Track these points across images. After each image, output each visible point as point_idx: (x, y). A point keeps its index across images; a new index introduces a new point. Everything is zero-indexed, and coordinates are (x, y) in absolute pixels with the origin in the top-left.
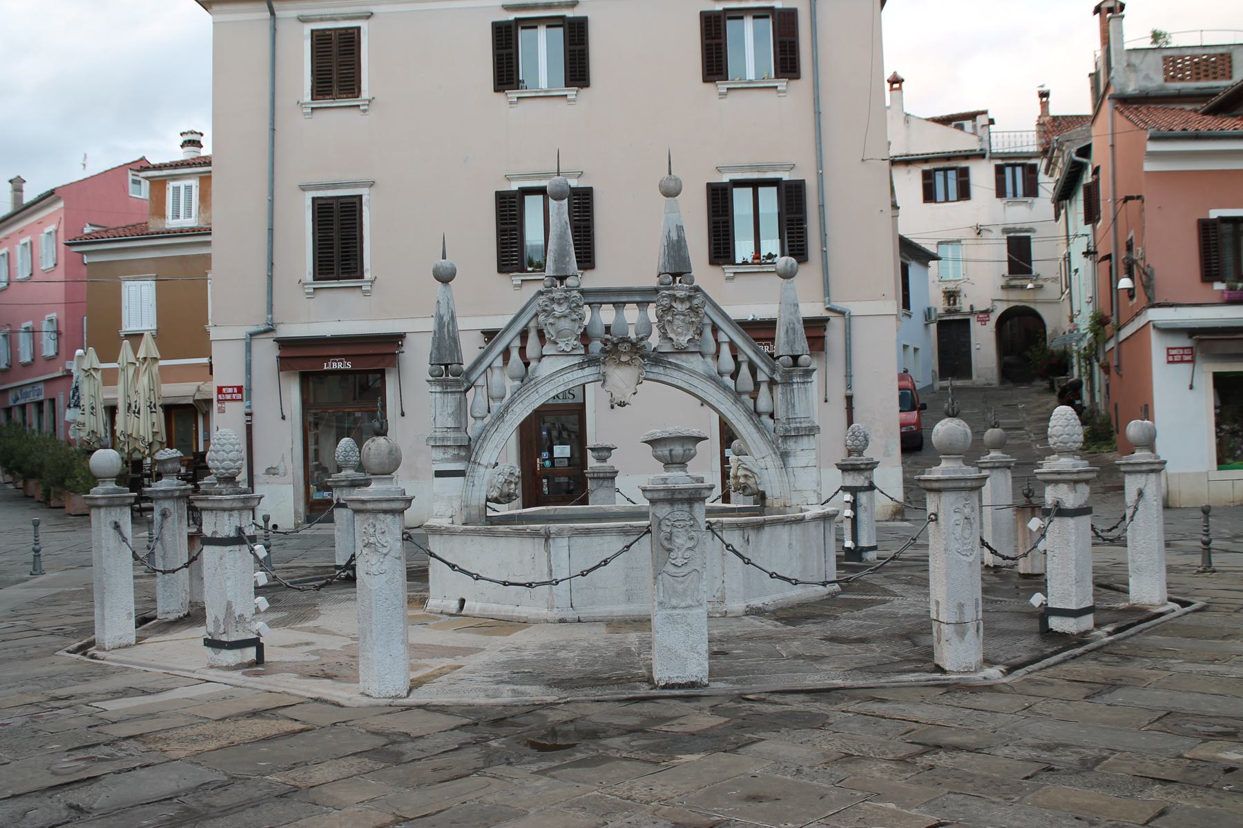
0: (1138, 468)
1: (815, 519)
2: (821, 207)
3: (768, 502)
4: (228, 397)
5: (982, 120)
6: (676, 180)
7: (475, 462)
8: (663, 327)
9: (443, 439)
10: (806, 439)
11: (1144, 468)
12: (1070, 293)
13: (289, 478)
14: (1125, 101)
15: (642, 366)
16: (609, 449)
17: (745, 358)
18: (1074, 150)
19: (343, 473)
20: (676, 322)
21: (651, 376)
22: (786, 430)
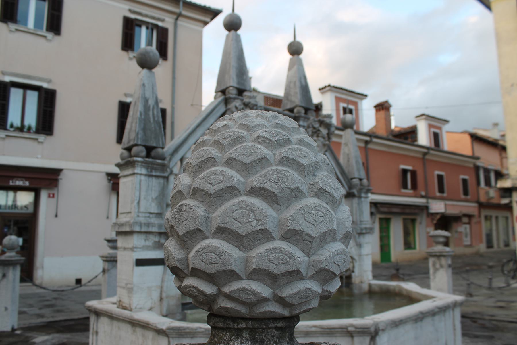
9: (148, 225)
22: (362, 229)
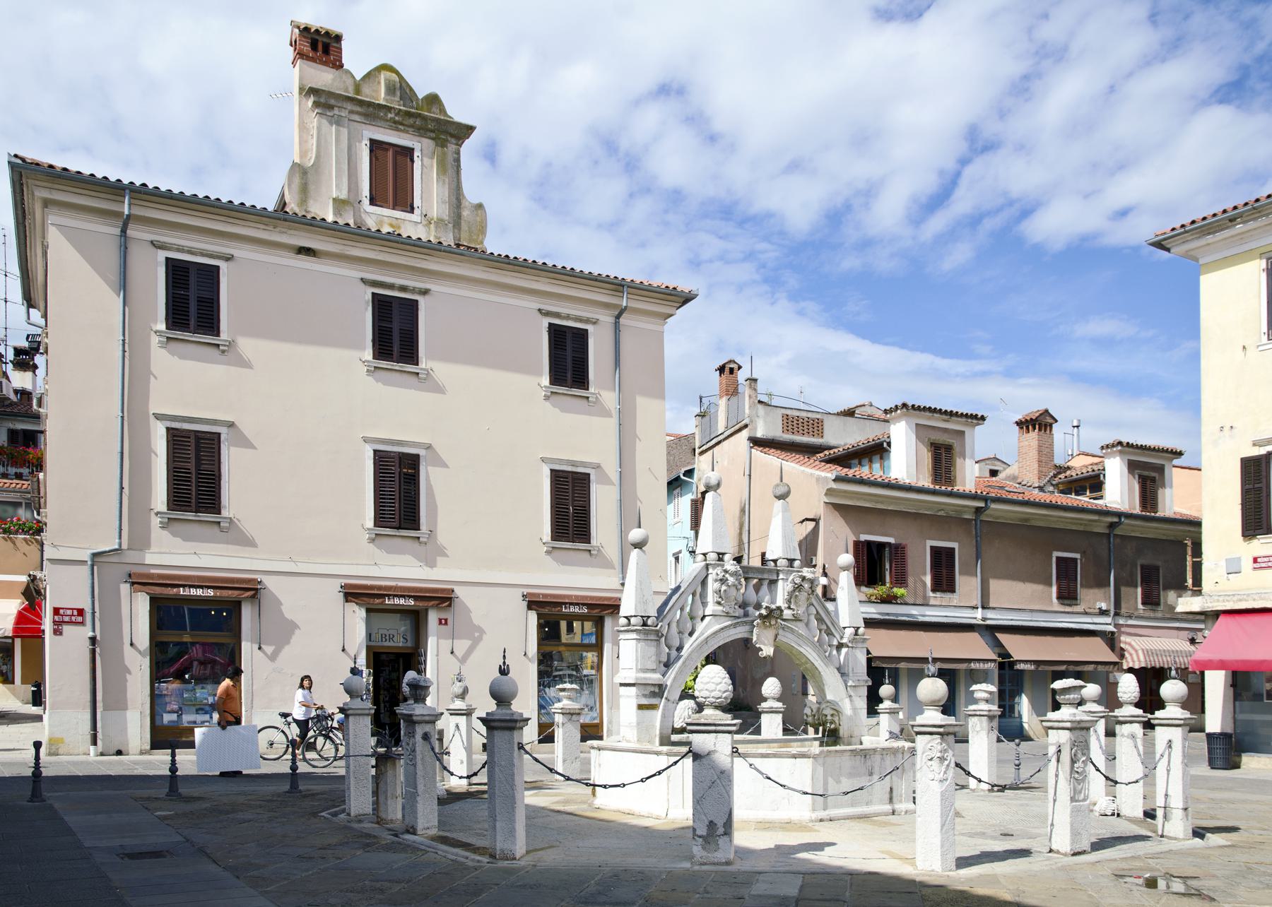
18: (683, 470)
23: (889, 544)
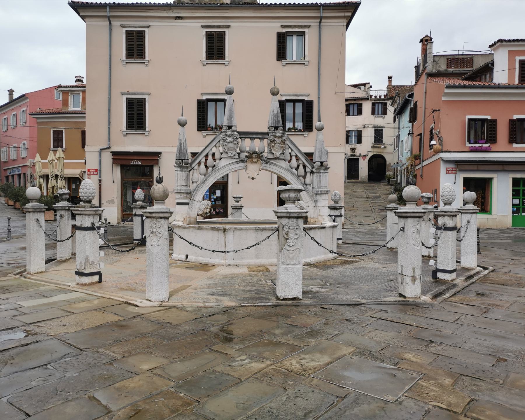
0: (468, 211)
1: (330, 227)
2: (319, 110)
3: (309, 219)
4: (92, 173)
5: (367, 86)
6: (277, 89)
7: (193, 200)
8: (270, 148)
9: (180, 190)
10: (325, 195)
11: (471, 211)
12: (399, 149)
13: (115, 204)
14: (431, 75)
15: (261, 164)
16: (240, 198)
17: (302, 162)
18: (407, 95)
19: (138, 203)
20: (276, 147)
21: (264, 168)
23: (486, 119)
